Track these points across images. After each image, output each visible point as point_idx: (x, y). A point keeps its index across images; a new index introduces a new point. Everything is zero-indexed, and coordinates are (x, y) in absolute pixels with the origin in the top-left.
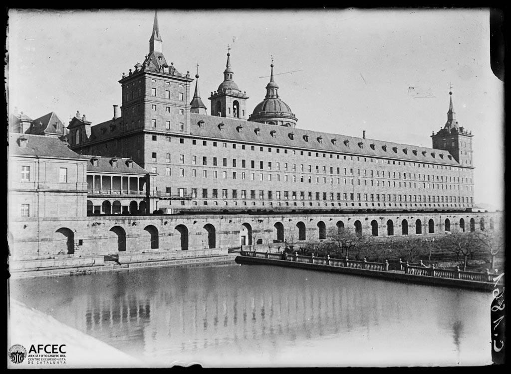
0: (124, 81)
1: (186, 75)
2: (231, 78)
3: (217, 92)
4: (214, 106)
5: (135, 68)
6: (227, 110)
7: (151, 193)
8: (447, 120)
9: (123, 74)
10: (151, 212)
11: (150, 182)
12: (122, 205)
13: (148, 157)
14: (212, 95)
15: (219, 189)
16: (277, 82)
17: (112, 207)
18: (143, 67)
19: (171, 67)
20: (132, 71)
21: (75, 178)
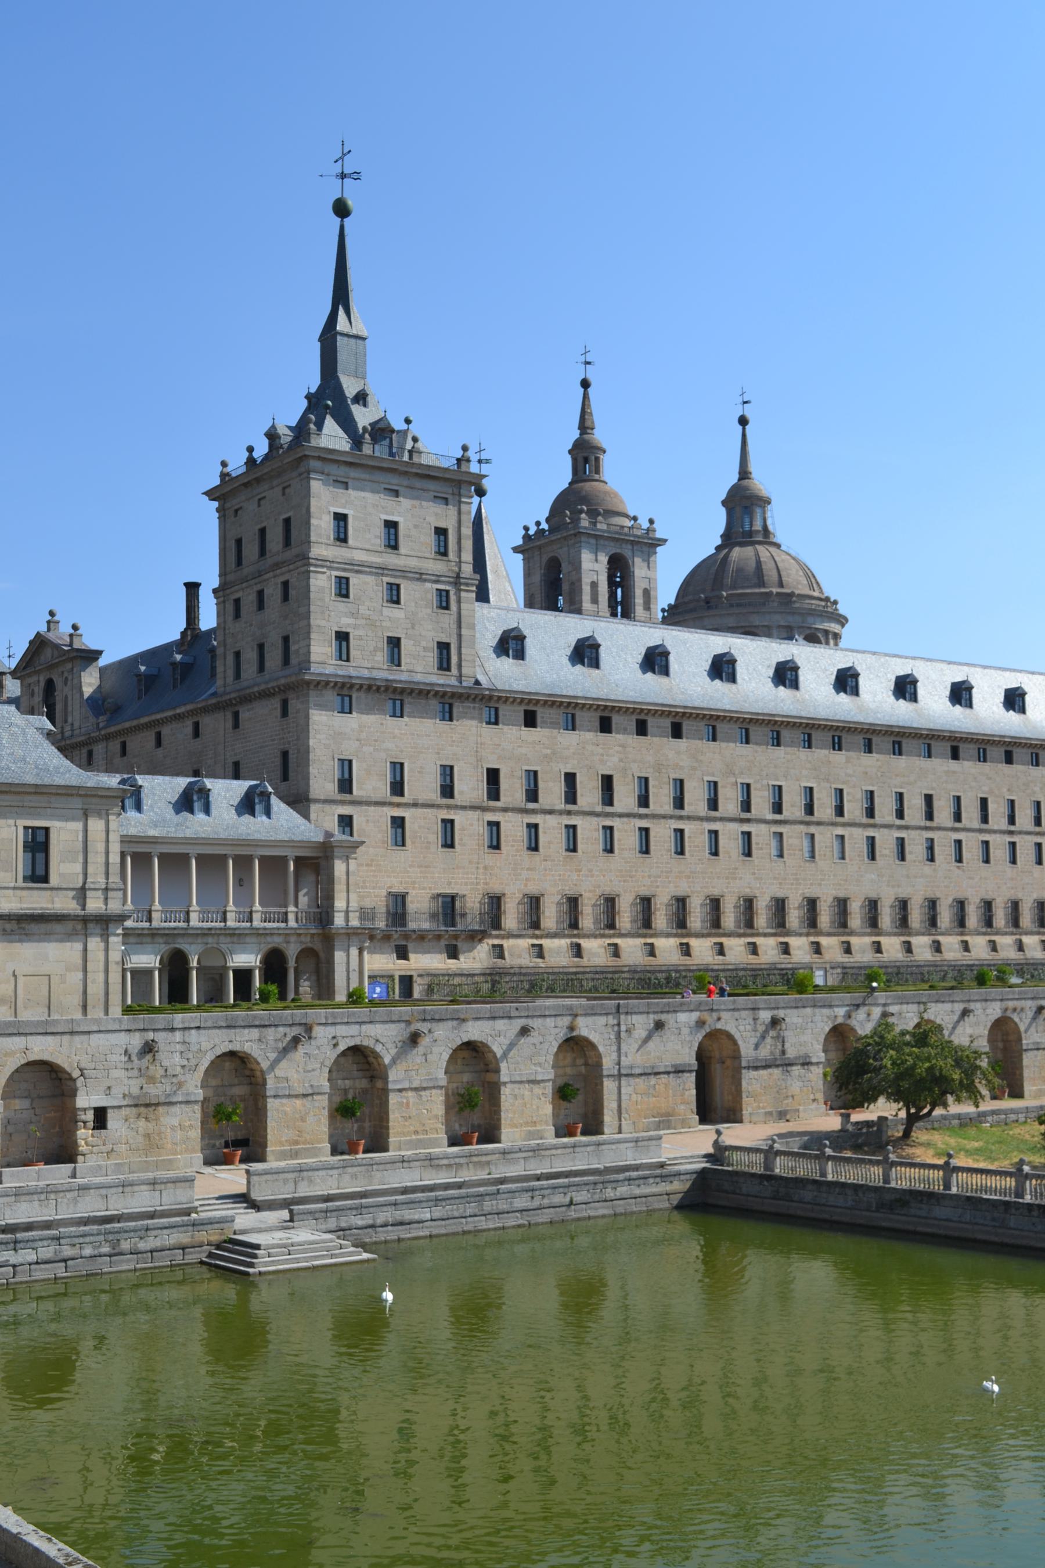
0: (227, 494)
1: (459, 460)
2: (597, 472)
3: (545, 526)
4: (537, 578)
5: (266, 441)
6: (586, 589)
7: (339, 920)
9: (224, 464)
10: (341, 997)
11: (337, 873)
12: (230, 964)
13: (322, 781)
14: (527, 537)
15: (586, 895)
16: (762, 481)
17: (194, 972)
18: (301, 431)
19: (405, 432)
20: (255, 455)
21: (78, 868)
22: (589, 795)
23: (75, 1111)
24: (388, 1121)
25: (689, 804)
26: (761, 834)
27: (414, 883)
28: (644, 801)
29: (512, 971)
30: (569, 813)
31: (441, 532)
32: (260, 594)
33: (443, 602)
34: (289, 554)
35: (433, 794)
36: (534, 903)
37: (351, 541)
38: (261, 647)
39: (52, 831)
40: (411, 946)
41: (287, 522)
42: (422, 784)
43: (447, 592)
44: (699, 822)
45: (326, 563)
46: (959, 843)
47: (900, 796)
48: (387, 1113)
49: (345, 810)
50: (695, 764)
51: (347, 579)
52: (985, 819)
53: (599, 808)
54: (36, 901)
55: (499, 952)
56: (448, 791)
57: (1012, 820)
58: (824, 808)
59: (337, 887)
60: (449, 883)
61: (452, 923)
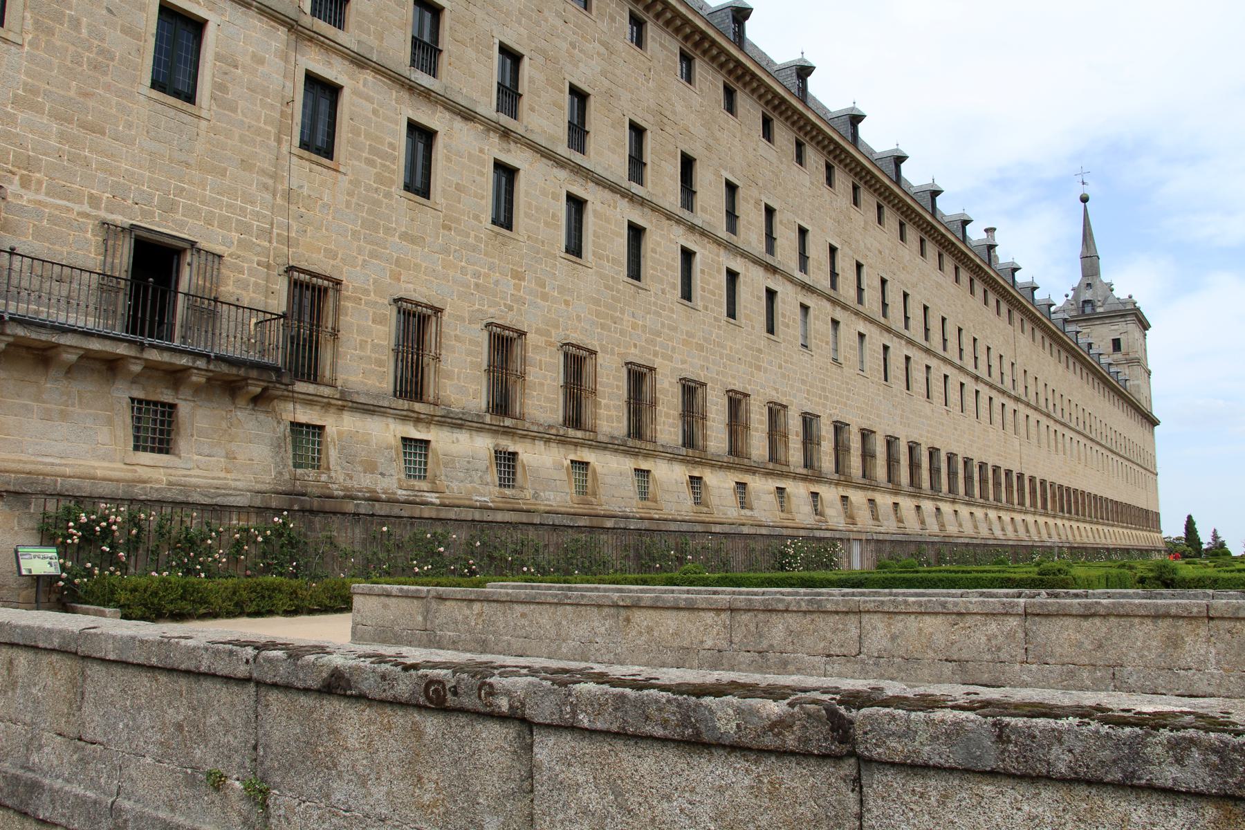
15: (531, 338)
25: (704, 210)
27: (30, 164)
29: (350, 507)
30: (506, 134)
44: (714, 247)
50: (710, 141)
60: (169, 207)
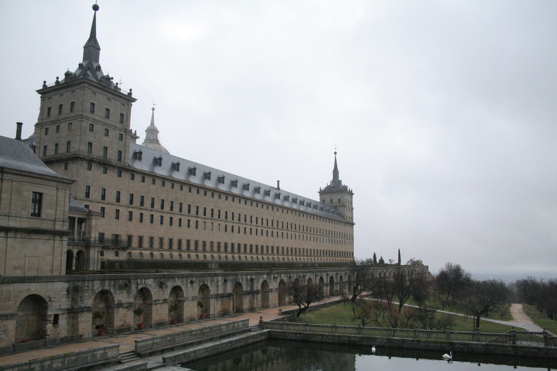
0: (45, 92)
8: (332, 178)
9: (45, 82)
15: (155, 237)
21: (52, 211)
22: (157, 206)
23: (46, 315)
24: (151, 316)
26: (200, 221)
28: (172, 209)
30: (152, 210)
31: (122, 115)
32: (58, 127)
33: (121, 138)
34: (73, 114)
35: (114, 201)
36: (141, 239)
37: (95, 113)
38: (57, 145)
39: (44, 195)
40: (105, 252)
41: (73, 104)
42: (111, 196)
43: (122, 135)
45: (88, 118)
46: (245, 228)
47: (233, 213)
48: (152, 314)
49: (87, 203)
51: (93, 125)
52: (251, 222)
53: (160, 210)
54: (35, 224)
55: (130, 253)
56: (118, 200)
57: (257, 223)
58: (216, 216)
59: (92, 229)
61: (116, 244)
